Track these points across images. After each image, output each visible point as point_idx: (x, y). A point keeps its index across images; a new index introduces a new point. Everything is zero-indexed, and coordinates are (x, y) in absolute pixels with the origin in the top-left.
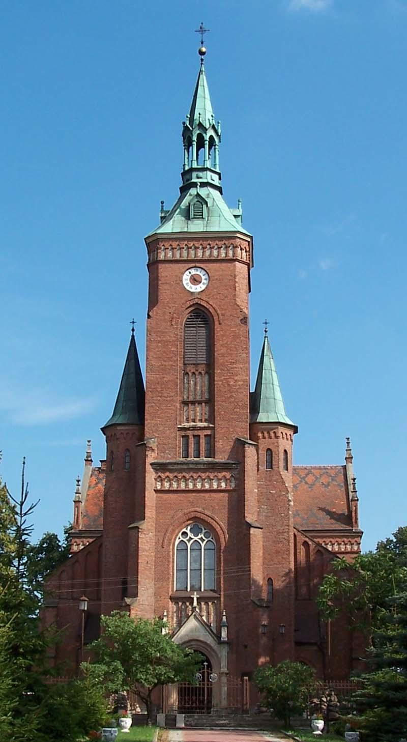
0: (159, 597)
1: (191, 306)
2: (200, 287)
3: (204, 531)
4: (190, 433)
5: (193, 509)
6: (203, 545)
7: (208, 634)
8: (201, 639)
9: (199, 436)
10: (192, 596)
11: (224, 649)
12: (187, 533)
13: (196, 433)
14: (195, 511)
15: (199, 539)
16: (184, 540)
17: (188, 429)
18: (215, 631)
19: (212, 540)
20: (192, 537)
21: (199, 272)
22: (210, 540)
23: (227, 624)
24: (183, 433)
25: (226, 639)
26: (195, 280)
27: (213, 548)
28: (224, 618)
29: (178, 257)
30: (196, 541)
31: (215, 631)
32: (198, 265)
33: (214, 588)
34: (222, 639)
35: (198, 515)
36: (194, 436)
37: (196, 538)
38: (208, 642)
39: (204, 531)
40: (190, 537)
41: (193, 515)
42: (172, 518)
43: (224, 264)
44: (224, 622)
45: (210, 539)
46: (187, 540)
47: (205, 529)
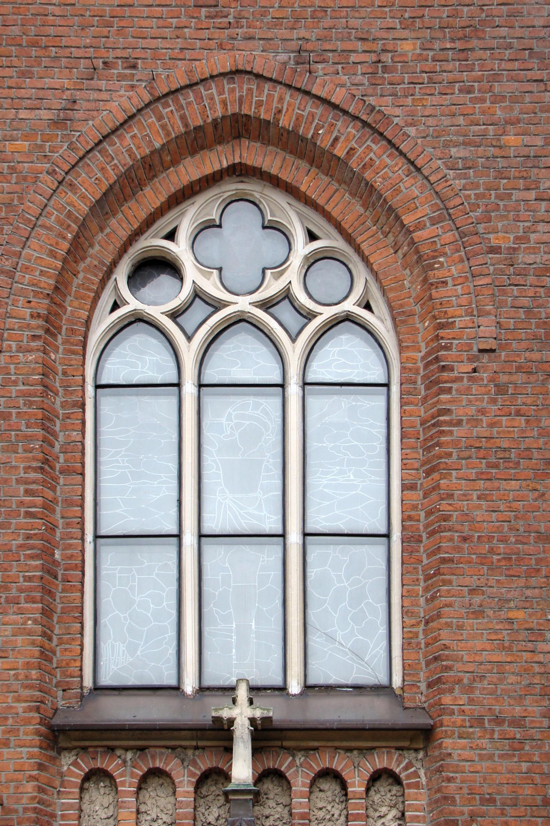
3: (302, 248)
5: (222, 61)
6: (294, 353)
10: (225, 714)
12: (168, 266)
14: (236, 73)
16: (156, 312)
20: (212, 287)
22: (348, 318)
30: (241, 319)
33: (383, 679)
35: (263, 102)
37: (243, 304)
40: (198, 294)
41: (216, 103)
42: (57, 123)
45: (349, 306)
46: (174, 315)
47: (312, 237)
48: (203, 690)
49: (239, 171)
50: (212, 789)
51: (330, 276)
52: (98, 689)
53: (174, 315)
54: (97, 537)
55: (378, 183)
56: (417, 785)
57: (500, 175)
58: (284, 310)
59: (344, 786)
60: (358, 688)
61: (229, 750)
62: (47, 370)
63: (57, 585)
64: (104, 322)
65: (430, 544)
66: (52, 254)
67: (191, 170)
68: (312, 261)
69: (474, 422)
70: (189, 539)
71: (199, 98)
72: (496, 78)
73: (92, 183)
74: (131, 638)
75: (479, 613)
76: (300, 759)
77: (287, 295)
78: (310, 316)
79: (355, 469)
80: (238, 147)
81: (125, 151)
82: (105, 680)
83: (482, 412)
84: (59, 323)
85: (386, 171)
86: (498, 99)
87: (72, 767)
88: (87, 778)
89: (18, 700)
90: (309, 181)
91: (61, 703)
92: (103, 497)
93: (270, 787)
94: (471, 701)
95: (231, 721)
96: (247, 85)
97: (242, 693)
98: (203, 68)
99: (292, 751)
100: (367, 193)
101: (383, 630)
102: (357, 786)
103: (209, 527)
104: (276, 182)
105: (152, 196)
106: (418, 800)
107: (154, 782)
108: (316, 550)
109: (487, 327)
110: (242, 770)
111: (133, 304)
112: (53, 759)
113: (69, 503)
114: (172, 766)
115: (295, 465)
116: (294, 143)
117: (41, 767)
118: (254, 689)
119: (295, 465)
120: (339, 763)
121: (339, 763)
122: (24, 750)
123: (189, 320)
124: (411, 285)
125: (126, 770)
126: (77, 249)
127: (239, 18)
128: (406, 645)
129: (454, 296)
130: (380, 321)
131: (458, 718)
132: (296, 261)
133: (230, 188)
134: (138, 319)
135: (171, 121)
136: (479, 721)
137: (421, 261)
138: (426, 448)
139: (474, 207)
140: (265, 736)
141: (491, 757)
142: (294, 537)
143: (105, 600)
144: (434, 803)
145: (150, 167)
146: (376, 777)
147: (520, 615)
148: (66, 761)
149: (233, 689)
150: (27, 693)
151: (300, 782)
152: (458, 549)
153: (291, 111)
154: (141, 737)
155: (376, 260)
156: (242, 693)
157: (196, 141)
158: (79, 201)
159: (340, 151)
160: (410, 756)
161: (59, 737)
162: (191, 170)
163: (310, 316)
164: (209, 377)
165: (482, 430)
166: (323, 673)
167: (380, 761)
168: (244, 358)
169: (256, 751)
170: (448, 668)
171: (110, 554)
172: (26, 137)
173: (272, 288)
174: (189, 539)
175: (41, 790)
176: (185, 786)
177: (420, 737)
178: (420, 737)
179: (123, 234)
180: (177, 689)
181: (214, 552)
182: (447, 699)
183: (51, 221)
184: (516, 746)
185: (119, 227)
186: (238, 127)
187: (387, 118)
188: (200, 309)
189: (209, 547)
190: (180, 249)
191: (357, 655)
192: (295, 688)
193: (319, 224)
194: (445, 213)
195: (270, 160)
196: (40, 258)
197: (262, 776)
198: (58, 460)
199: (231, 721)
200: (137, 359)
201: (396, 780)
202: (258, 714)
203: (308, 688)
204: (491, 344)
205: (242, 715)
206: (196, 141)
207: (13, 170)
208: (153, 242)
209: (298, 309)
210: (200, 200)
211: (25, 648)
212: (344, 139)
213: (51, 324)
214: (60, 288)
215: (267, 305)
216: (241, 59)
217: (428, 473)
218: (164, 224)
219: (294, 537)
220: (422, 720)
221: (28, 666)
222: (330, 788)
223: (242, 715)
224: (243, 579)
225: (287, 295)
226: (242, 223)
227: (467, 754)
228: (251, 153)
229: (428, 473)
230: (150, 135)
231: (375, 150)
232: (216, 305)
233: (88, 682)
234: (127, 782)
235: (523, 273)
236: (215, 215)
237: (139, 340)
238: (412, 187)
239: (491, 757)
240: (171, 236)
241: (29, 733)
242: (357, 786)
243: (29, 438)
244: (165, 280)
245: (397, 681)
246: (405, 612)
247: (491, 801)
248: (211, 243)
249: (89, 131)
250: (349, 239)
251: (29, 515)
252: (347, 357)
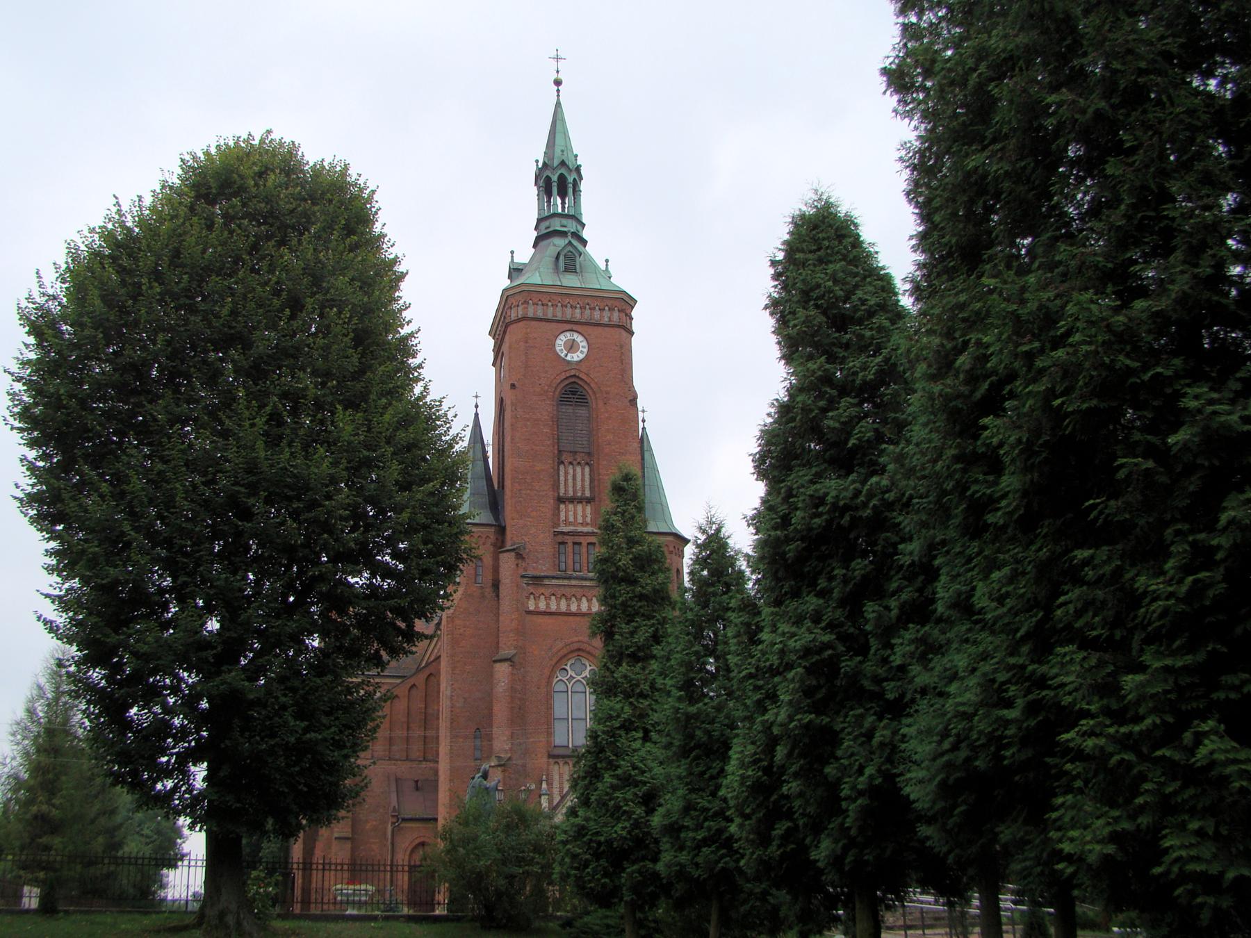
1: (567, 378)
2: (576, 357)
4: (570, 540)
5: (576, 639)
9: (580, 544)
13: (577, 539)
17: (568, 534)
21: (579, 339)
24: (560, 538)
26: (572, 346)
29: (550, 316)
32: (574, 327)
36: (575, 543)
39: (589, 668)
41: (576, 646)
43: (607, 329)
73: (555, 660)
81: (561, 654)
116: (589, 653)
122: (545, 759)
125: (560, 761)
153: (589, 648)
157: (572, 652)
158: (553, 663)
186: (579, 650)
198: (549, 708)
206: (572, 652)
226: (578, 665)
230: (565, 651)
249: (554, 650)
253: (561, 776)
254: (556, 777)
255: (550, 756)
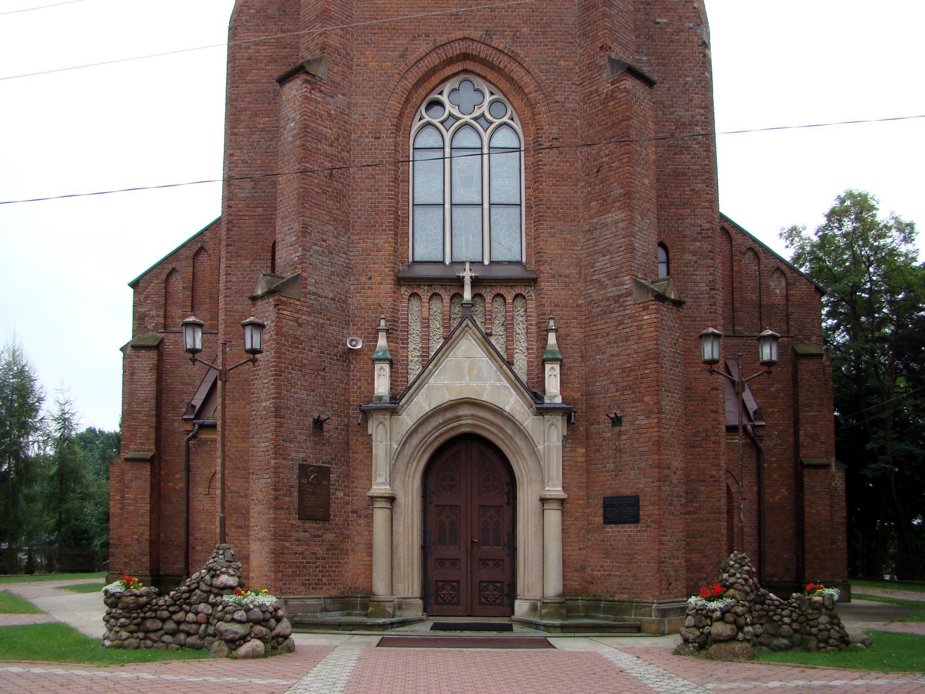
0: (364, 279)
3: (488, 98)
5: (459, 34)
7: (505, 383)
8: (485, 397)
10: (461, 275)
11: (553, 428)
12: (441, 104)
14: (464, 39)
15: (475, 119)
18: (524, 378)
19: (510, 122)
20: (456, 113)
22: (505, 124)
23: (560, 357)
25: (558, 400)
27: (515, 144)
28: (552, 339)
31: (524, 378)
33: (518, 259)
34: (547, 400)
35: (474, 48)
37: (467, 118)
38: (507, 409)
40: (450, 115)
41: (457, 49)
42: (401, 56)
44: (553, 352)
45: (505, 119)
46: (442, 123)
47: (492, 94)
48: (452, 263)
49: (465, 71)
50: (456, 300)
51: (498, 108)
52: (414, 262)
53: (442, 123)
54: (413, 205)
55: (515, 77)
56: (531, 300)
57: (559, 76)
58: (482, 121)
59: (505, 299)
60: (510, 263)
61: (463, 286)
62: (396, 144)
63: (399, 225)
64: (417, 125)
65: (537, 210)
66: (399, 103)
67: (448, 71)
68: (492, 103)
69: (551, 165)
70: (447, 206)
71: (451, 47)
72: (556, 41)
73: (413, 77)
74: (426, 244)
75: (553, 236)
76: (488, 290)
77: (483, 115)
78: (491, 123)
79: (508, 178)
80: (466, 63)
81: (425, 66)
82: (417, 259)
83: (554, 161)
84: (401, 127)
85: (518, 73)
86: (556, 49)
87: (405, 291)
88: (411, 296)
89: (386, 267)
90: (491, 75)
91: (401, 268)
92: (416, 190)
93: (477, 299)
94: (551, 269)
95: (463, 277)
96: (469, 43)
97: (467, 266)
98: (453, 36)
99: (485, 287)
100: (512, 81)
101: (519, 240)
102: (509, 300)
103: (455, 201)
104: (479, 75)
105: (434, 80)
106: (532, 305)
107: (435, 298)
108: (494, 210)
109: (555, 130)
110: (467, 295)
111: (427, 119)
112: (398, 289)
113: (403, 193)
114: (442, 292)
115: (485, 179)
116: (485, 62)
117: (394, 292)
118: (472, 263)
119: (485, 179)
120: (502, 291)
121: (502, 291)
123: (447, 124)
124: (527, 113)
125: (425, 293)
126: (408, 100)
127: (465, 19)
128: (528, 247)
129: (543, 118)
130: (517, 126)
131: (546, 275)
132: (486, 103)
133: (463, 77)
134: (429, 124)
135: (442, 55)
136: (554, 277)
137: (531, 105)
138: (534, 174)
139: (550, 87)
140: (475, 282)
141: (558, 289)
142: (486, 206)
143: (416, 228)
144: (537, 307)
145: (434, 71)
146: (516, 296)
147: (568, 236)
148: (403, 289)
149: (463, 263)
150: (389, 265)
151: (488, 298)
152: (546, 212)
153: (484, 52)
154: (431, 281)
155: (515, 104)
156: (467, 266)
157: (450, 61)
158: (408, 84)
159: (502, 66)
160: (529, 288)
161: (401, 281)
162: (448, 71)
163: (491, 123)
164: (455, 145)
165: (554, 167)
166: (497, 257)
167: (518, 290)
168: (467, 139)
169: (473, 287)
170: (542, 257)
171: (418, 210)
172: (390, 61)
173: (477, 113)
174: (447, 206)
175: (394, 301)
176: (447, 300)
177: (532, 282)
178: (532, 282)
179: (424, 94)
180: (443, 262)
181: (458, 211)
182: (542, 268)
183: (399, 91)
184: (567, 285)
185: (422, 91)
186: (465, 57)
187: (518, 55)
188: (451, 120)
189: (455, 209)
190: (444, 98)
191: (509, 250)
192: (486, 262)
193: (494, 90)
194: (539, 88)
195: (477, 68)
196: (394, 104)
197: (473, 297)
199: (463, 277)
200: (428, 139)
201: (524, 298)
202: (473, 275)
203: (491, 262)
204: (556, 136)
205: (467, 275)
206: (450, 61)
207: (385, 73)
208: (435, 96)
209: (487, 120)
210: (451, 81)
211: (388, 248)
212: (502, 61)
213: (398, 127)
214: (401, 114)
215: (475, 119)
216: (466, 33)
217: (535, 183)
218: (439, 89)
219: (486, 206)
220: (534, 276)
221: (389, 255)
222: (500, 300)
223: (467, 275)
224: (468, 219)
225: (483, 115)
226: (466, 89)
227: (550, 288)
228: (470, 65)
229: (535, 183)
231: (513, 66)
232: (458, 119)
233: (411, 260)
234: (425, 298)
235: (567, 110)
236: (457, 87)
237: (429, 130)
238: (527, 79)
239: (558, 289)
240: (441, 93)
241: (390, 279)
242: (509, 300)
243: (390, 170)
244: (437, 108)
245: (524, 260)
246: (527, 235)
247: (558, 306)
248: (455, 96)
249: (412, 59)
250: (505, 95)
251: (390, 198)
252: (505, 138)
253: (426, 324)
254: (415, 327)
255: (401, 281)
